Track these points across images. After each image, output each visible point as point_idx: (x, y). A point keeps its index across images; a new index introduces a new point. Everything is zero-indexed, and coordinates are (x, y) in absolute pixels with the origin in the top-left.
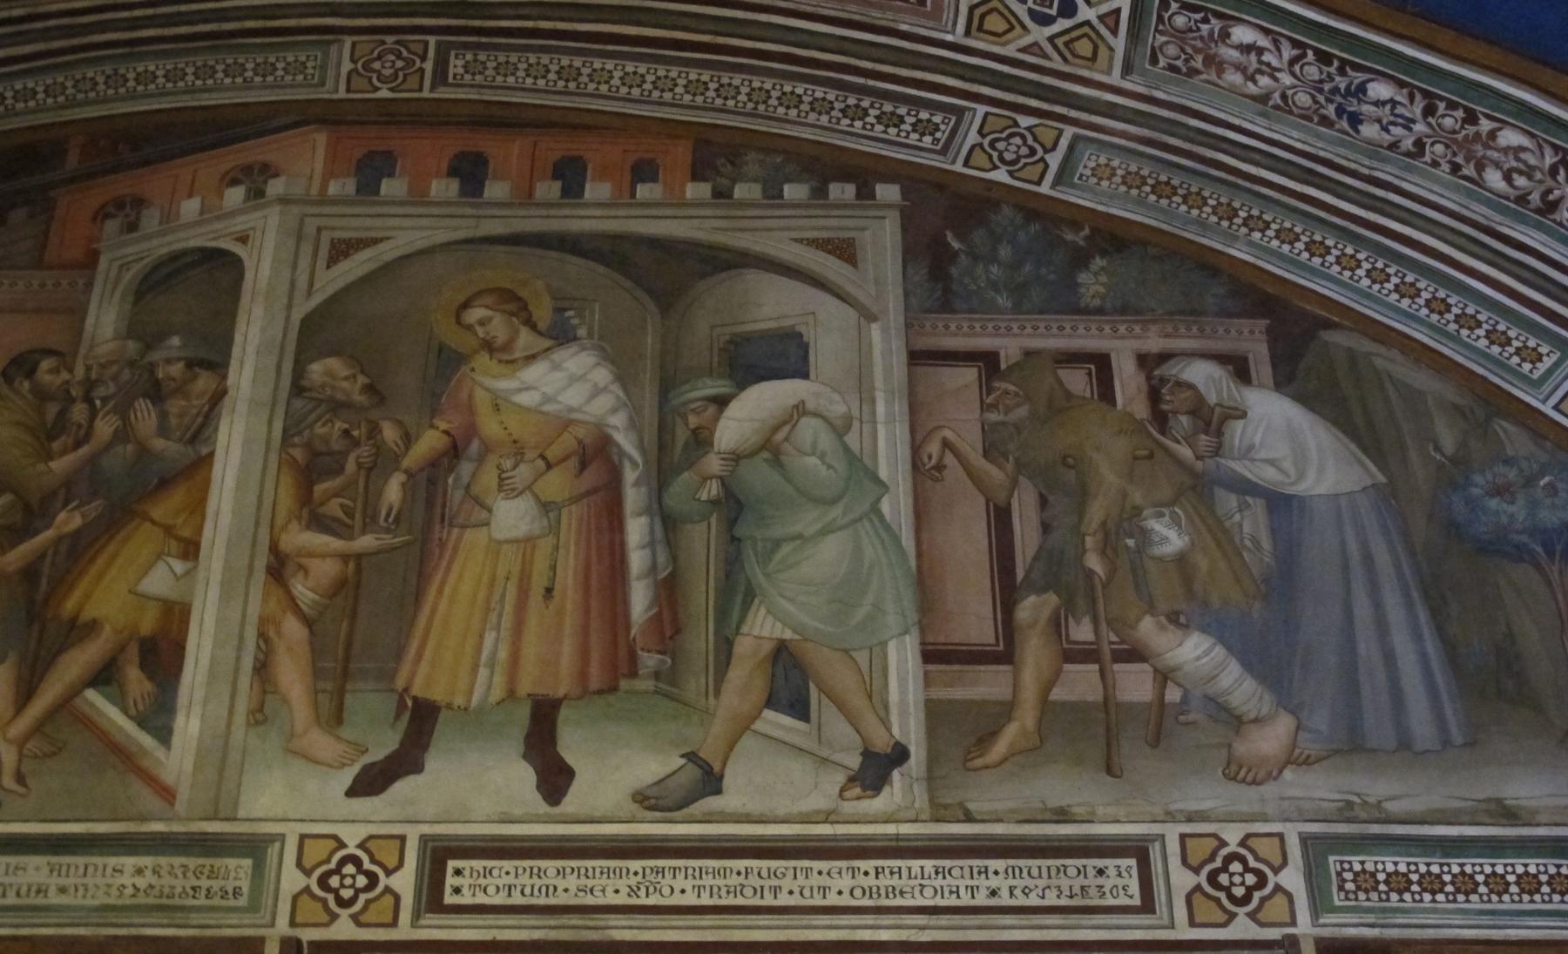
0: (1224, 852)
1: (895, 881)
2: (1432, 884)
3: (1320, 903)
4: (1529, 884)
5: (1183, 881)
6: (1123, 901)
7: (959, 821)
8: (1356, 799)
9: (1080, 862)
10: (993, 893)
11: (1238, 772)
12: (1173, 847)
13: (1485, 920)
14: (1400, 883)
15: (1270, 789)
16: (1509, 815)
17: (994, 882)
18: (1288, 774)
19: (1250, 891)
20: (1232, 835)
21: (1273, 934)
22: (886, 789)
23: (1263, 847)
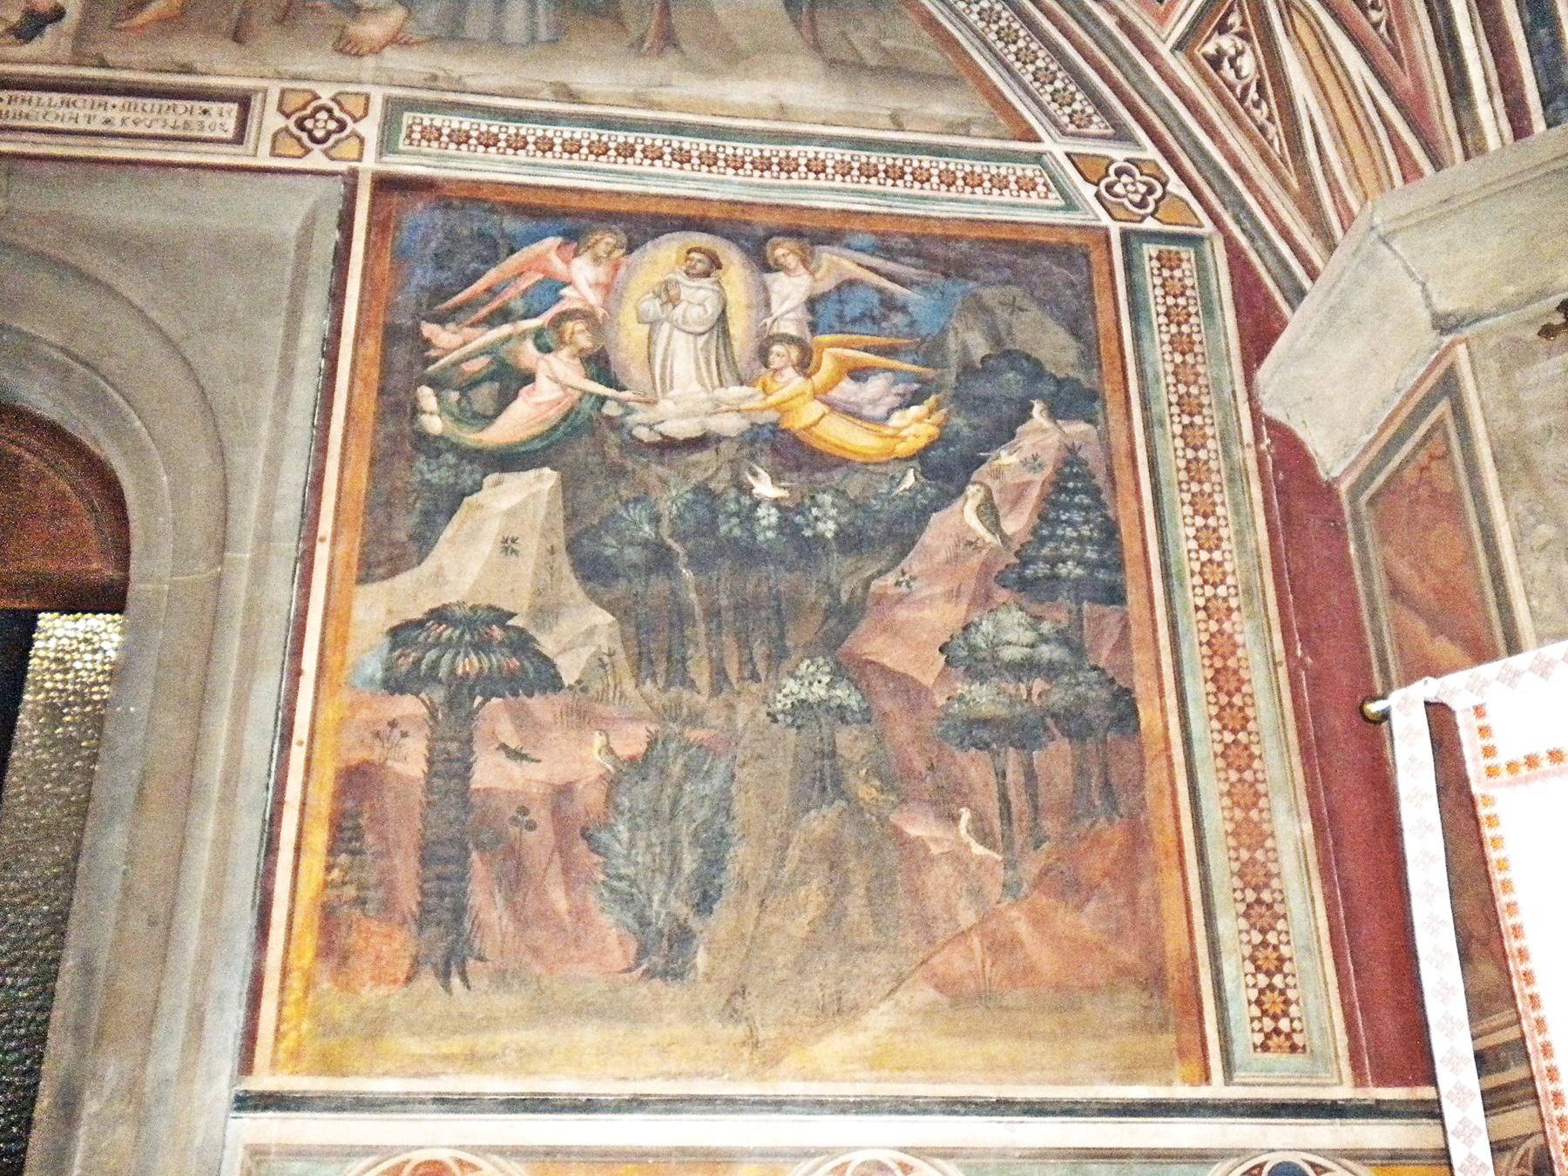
0: (314, 104)
1: (25, 109)
2: (489, 141)
3: (387, 145)
4: (572, 148)
5: (275, 122)
6: (219, 134)
7: (93, 66)
8: (441, 74)
9: (189, 104)
10: (107, 122)
11: (347, 47)
12: (273, 98)
13: (525, 170)
14: (461, 139)
15: (370, 62)
16: (572, 96)
17: (110, 114)
18: (388, 51)
19: (329, 134)
20: (326, 94)
21: (342, 167)
22: (38, 39)
23: (350, 104)
